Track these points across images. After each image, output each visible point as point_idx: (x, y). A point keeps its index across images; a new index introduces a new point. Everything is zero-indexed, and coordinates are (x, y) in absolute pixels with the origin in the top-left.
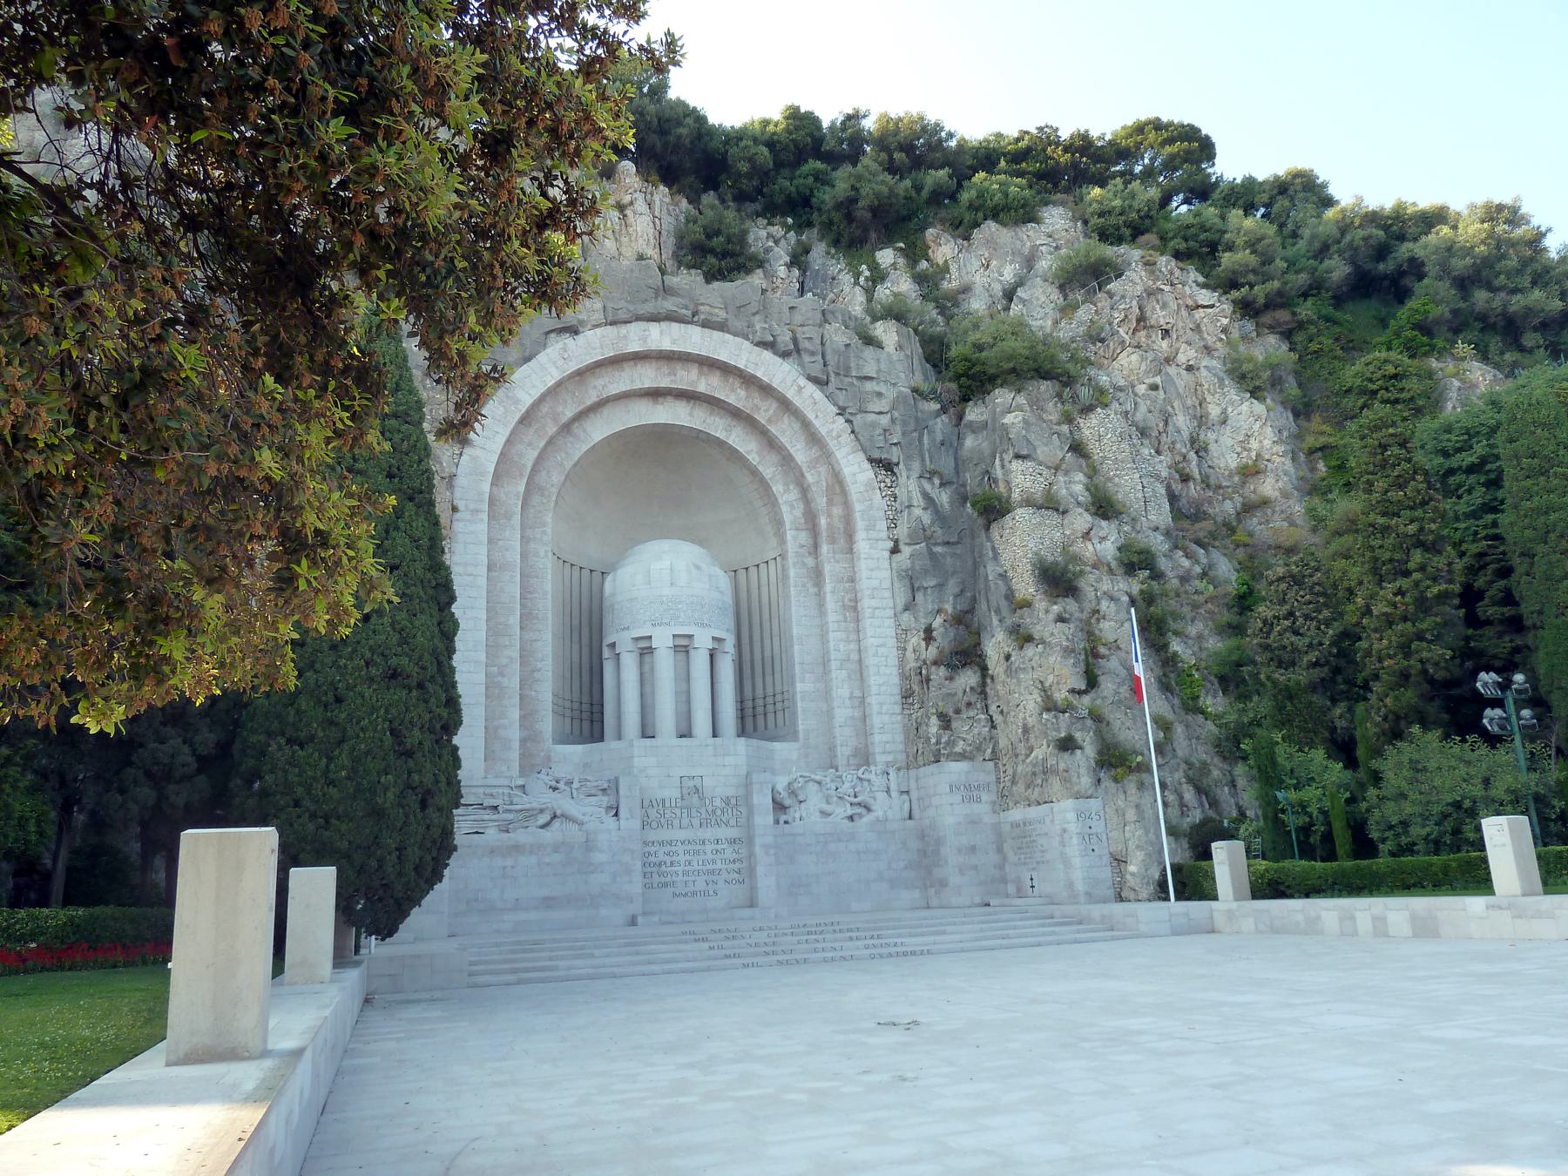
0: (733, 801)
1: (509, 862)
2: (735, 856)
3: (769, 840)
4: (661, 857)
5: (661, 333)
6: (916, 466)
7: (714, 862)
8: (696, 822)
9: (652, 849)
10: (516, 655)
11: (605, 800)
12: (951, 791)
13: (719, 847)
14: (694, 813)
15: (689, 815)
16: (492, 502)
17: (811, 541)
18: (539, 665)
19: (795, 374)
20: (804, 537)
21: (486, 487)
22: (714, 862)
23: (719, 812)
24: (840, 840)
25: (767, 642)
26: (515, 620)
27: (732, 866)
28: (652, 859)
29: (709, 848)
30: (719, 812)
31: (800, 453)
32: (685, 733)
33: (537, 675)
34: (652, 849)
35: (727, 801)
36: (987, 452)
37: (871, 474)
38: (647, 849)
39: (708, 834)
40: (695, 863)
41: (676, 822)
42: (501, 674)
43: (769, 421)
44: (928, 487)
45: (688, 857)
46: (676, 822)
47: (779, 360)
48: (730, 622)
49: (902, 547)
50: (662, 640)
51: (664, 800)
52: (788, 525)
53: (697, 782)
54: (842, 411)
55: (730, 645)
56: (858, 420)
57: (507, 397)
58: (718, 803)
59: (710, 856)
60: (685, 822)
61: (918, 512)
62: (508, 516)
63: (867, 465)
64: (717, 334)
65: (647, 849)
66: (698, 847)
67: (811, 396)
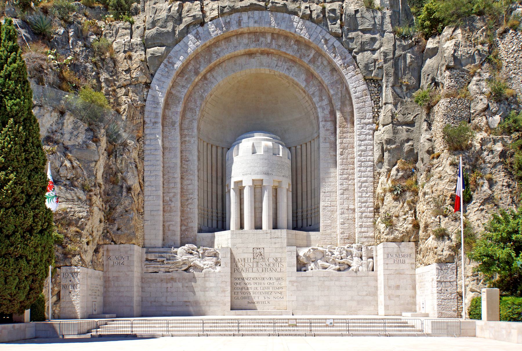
0: (279, 260)
1: (169, 285)
2: (279, 286)
3: (294, 278)
4: (243, 285)
5: (249, 18)
6: (392, 79)
7: (268, 288)
8: (260, 270)
9: (238, 282)
10: (179, 191)
11: (214, 259)
12: (388, 257)
13: (271, 281)
14: (260, 265)
15: (257, 266)
16: (164, 117)
17: (333, 128)
18: (191, 196)
19: (324, 32)
20: (329, 125)
21: (160, 111)
22: (268, 288)
23: (272, 265)
24: (332, 280)
25: (304, 184)
26: (178, 175)
27: (278, 290)
28: (238, 286)
29: (266, 281)
30: (272, 265)
31: (326, 79)
32: (258, 227)
33: (190, 201)
34: (238, 282)
35: (276, 260)
36: (435, 66)
37: (365, 87)
38: (236, 281)
39: (267, 275)
40: (259, 289)
41: (250, 270)
42: (171, 200)
43: (310, 62)
44: (398, 90)
45: (255, 286)
46: (250, 270)
47: (314, 25)
48: (288, 173)
49: (381, 127)
50: (247, 183)
51: (244, 259)
52: (320, 120)
53: (262, 250)
54: (351, 51)
55: (286, 184)
56: (359, 57)
57: (169, 63)
58: (271, 260)
59: (266, 285)
60: (255, 269)
61: (390, 106)
62: (173, 124)
63: (362, 81)
64: (279, 15)
65: (236, 281)
66: (260, 281)
67: (333, 45)
